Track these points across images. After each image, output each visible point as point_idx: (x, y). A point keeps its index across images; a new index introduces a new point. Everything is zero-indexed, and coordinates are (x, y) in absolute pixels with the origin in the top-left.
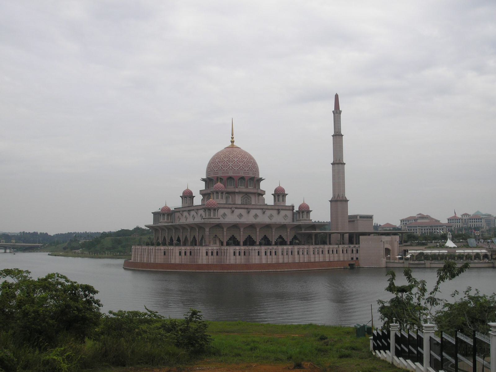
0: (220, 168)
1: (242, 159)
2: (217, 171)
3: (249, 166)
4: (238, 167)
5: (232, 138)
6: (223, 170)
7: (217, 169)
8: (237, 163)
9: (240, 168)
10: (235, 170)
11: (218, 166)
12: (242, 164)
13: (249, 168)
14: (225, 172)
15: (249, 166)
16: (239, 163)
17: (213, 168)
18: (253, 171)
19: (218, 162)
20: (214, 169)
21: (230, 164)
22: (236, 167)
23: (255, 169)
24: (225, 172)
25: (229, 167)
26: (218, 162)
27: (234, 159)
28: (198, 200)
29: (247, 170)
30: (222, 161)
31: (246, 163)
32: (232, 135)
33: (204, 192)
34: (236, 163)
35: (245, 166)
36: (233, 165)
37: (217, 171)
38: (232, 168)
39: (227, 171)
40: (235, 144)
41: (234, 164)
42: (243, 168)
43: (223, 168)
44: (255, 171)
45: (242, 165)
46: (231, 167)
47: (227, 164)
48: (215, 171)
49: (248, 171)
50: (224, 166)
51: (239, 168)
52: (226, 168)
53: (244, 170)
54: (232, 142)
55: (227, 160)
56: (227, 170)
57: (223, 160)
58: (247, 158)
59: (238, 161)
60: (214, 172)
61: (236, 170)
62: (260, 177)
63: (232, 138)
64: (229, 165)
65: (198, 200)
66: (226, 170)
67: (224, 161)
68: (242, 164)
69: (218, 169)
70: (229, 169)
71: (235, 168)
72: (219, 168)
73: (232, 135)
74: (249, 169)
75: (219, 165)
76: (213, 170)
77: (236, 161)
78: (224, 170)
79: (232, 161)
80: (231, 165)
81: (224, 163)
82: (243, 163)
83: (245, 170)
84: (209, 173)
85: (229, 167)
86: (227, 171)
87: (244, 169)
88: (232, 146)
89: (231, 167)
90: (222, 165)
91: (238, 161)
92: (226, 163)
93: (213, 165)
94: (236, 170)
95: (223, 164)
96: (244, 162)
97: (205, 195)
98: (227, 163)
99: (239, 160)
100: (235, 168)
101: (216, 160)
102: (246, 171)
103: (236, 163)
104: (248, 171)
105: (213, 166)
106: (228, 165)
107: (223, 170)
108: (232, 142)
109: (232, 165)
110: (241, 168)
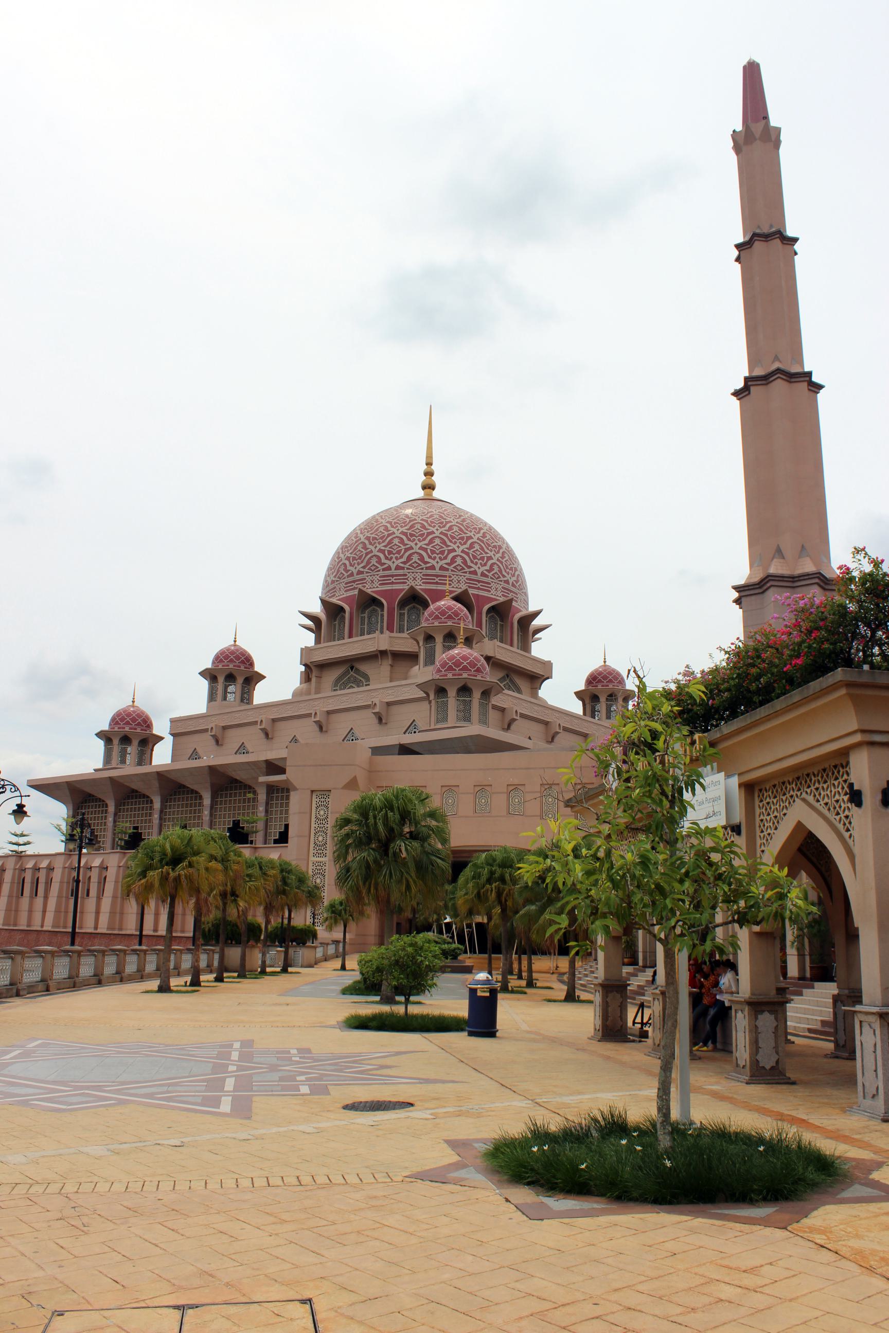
0: (374, 561)
1: (461, 530)
2: (359, 573)
3: (490, 558)
4: (445, 558)
5: (429, 474)
6: (384, 570)
7: (359, 567)
8: (444, 542)
9: (453, 560)
10: (433, 568)
11: (367, 554)
12: (462, 548)
13: (491, 569)
14: (392, 576)
15: (490, 558)
16: (449, 543)
17: (345, 564)
18: (507, 582)
19: (367, 542)
20: (349, 568)
21: (413, 544)
22: (438, 557)
23: (515, 578)
24: (392, 576)
25: (409, 559)
26: (367, 542)
27: (431, 529)
29: (483, 574)
30: (381, 538)
31: (477, 547)
32: (429, 464)
34: (437, 541)
35: (475, 557)
36: (425, 550)
37: (359, 573)
38: (422, 558)
39: (401, 572)
40: (436, 494)
41: (429, 547)
42: (465, 562)
43: (384, 560)
44: (513, 585)
45: (463, 551)
46: (415, 558)
47: (403, 547)
48: (352, 574)
49: (487, 576)
50: (390, 552)
51: (448, 560)
52: (397, 559)
53: (470, 573)
54: (428, 487)
55: (402, 533)
56: (403, 568)
57: (386, 533)
58: (482, 532)
59: (446, 535)
60: (351, 579)
61: (437, 567)
62: (532, 608)
63: (429, 474)
64: (411, 548)
66: (398, 568)
67: (389, 535)
68: (462, 548)
69: (364, 567)
70: (407, 566)
71: (434, 562)
72: (368, 562)
73: (429, 464)
74: (489, 571)
75: (372, 551)
76: (346, 575)
77: (437, 534)
78: (389, 568)
79: (422, 535)
80: (416, 549)
81: (390, 542)
82: (468, 545)
83: (475, 573)
84: (332, 586)
86: (401, 572)
87: (470, 567)
88: (429, 499)
89: (415, 558)
90: (380, 551)
91: (446, 535)
92: (396, 541)
94: (437, 567)
95: (385, 546)
96: (470, 542)
98: (402, 541)
99: (449, 533)
100: (434, 562)
101: (361, 536)
102: (479, 577)
103: (437, 541)
104: (487, 576)
105: (348, 559)
106: (406, 550)
107: (384, 570)
108: (428, 487)
109: (421, 548)
110: (459, 561)
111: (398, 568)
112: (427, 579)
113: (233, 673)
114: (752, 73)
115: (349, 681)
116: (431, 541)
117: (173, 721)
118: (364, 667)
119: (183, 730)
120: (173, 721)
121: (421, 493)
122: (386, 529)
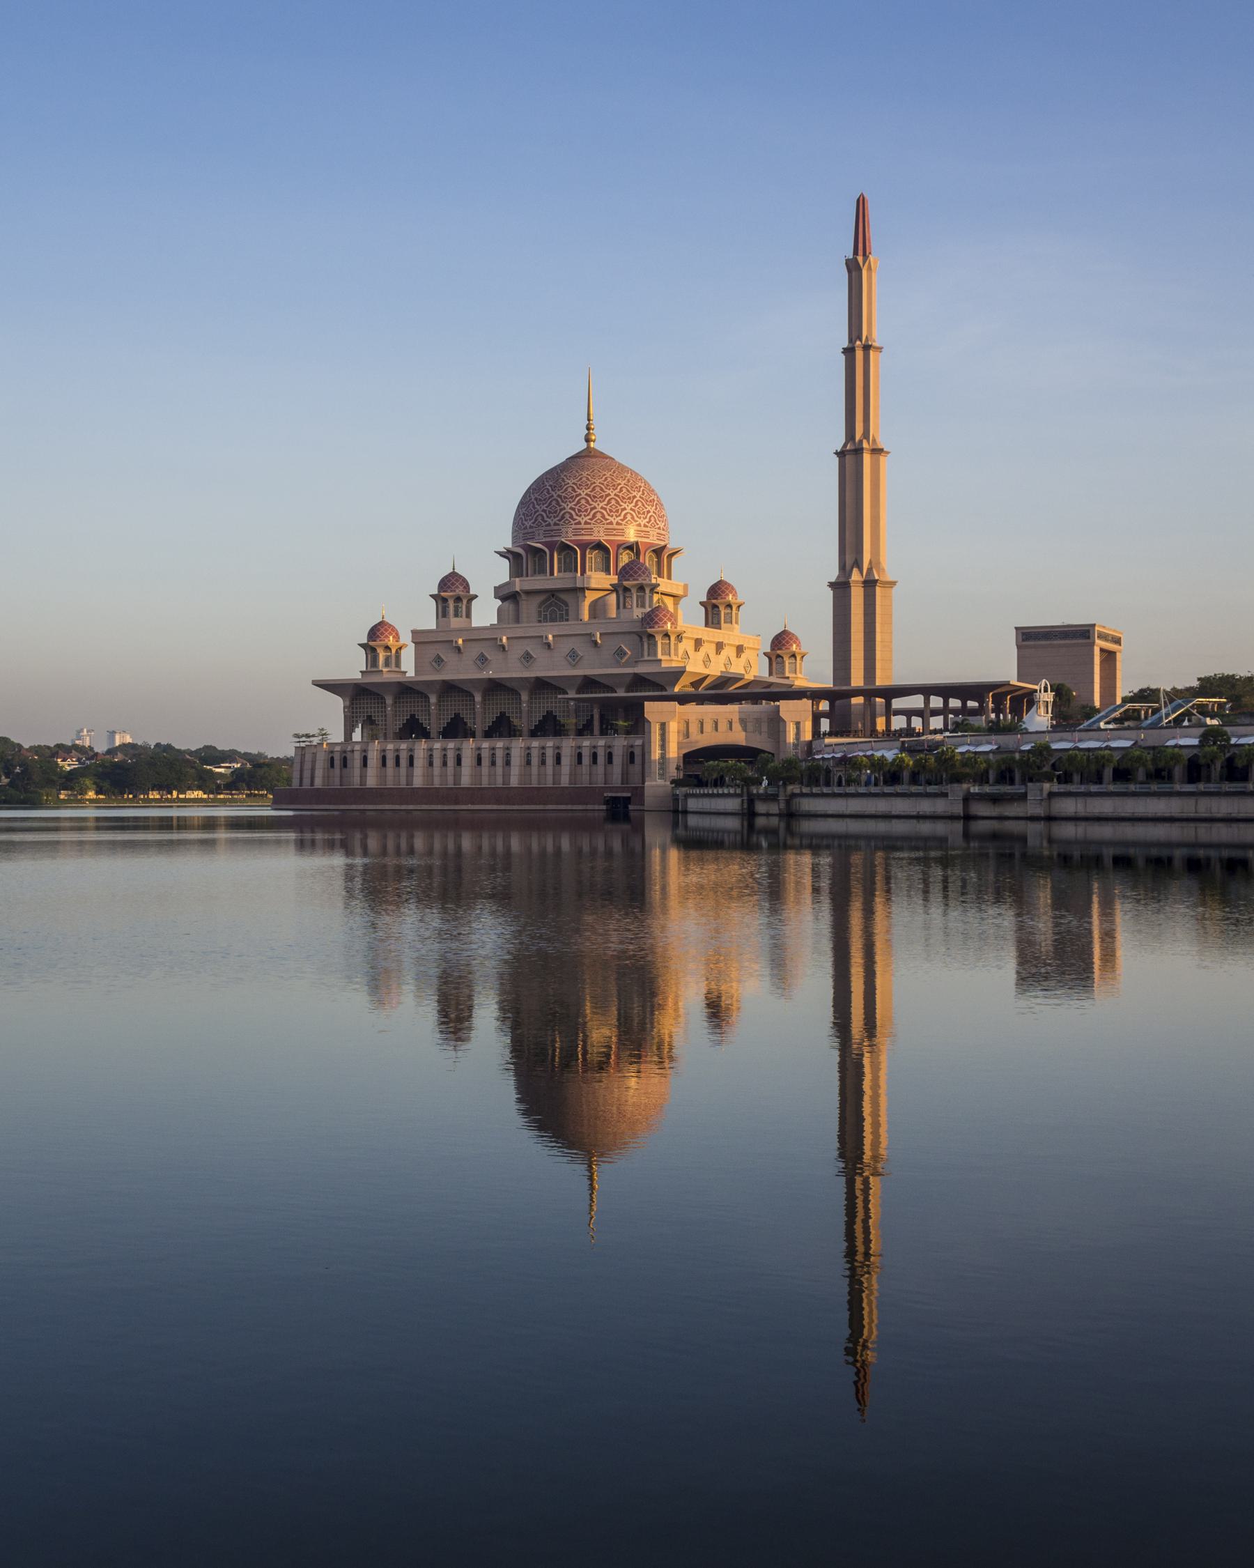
10: (611, 523)
25: (594, 516)
28: (485, 613)
33: (505, 592)
34: (613, 502)
37: (555, 524)
38: (603, 516)
46: (599, 516)
65: (485, 613)
80: (599, 509)
81: (579, 502)
85: (594, 516)
93: (544, 507)
97: (507, 595)
98: (587, 502)
108: (588, 440)
111: (586, 523)
112: (608, 532)
113: (453, 595)
114: (861, 203)
115: (551, 605)
116: (609, 502)
117: (414, 632)
118: (563, 596)
119: (420, 638)
120: (414, 632)
121: (584, 445)
122: (574, 490)
